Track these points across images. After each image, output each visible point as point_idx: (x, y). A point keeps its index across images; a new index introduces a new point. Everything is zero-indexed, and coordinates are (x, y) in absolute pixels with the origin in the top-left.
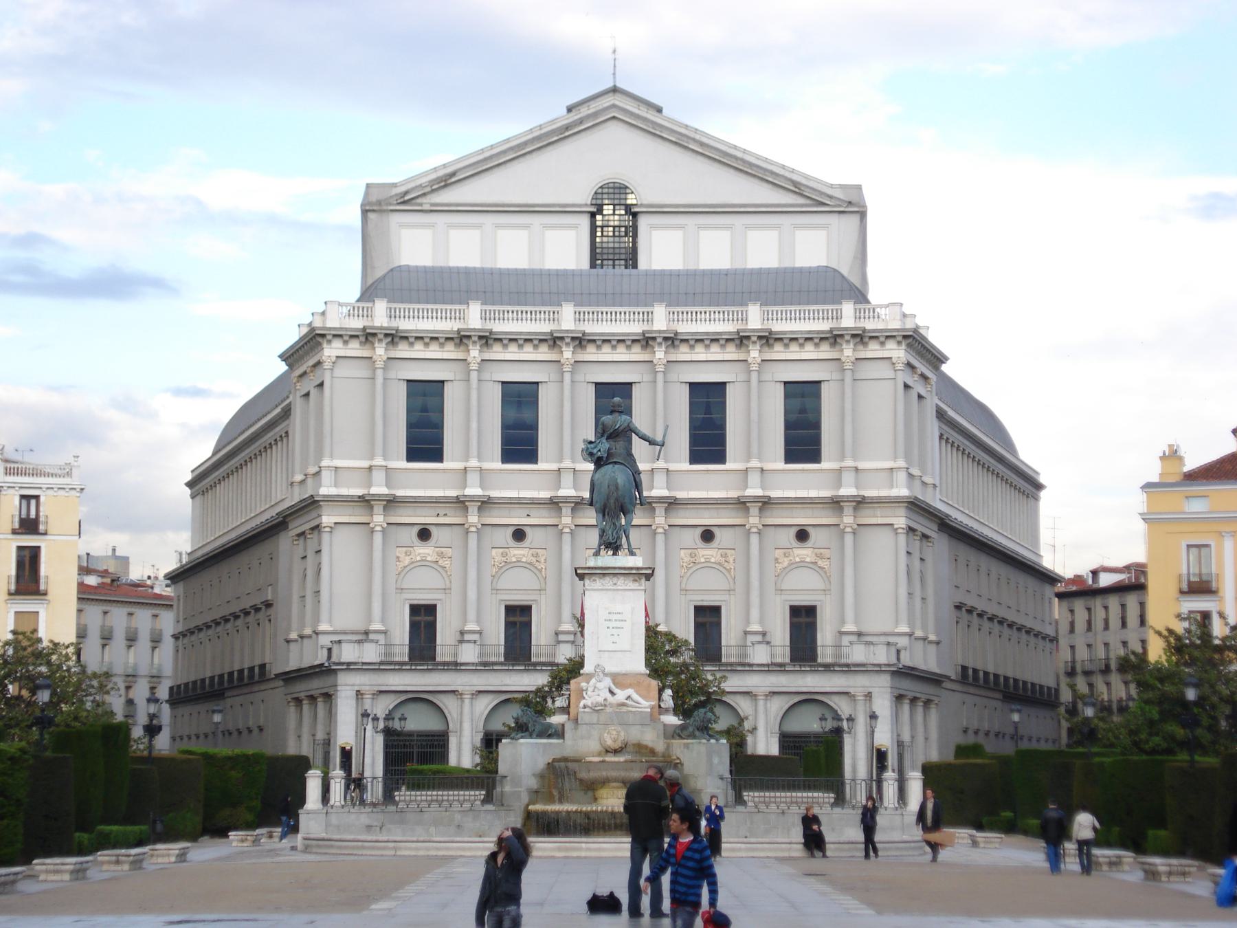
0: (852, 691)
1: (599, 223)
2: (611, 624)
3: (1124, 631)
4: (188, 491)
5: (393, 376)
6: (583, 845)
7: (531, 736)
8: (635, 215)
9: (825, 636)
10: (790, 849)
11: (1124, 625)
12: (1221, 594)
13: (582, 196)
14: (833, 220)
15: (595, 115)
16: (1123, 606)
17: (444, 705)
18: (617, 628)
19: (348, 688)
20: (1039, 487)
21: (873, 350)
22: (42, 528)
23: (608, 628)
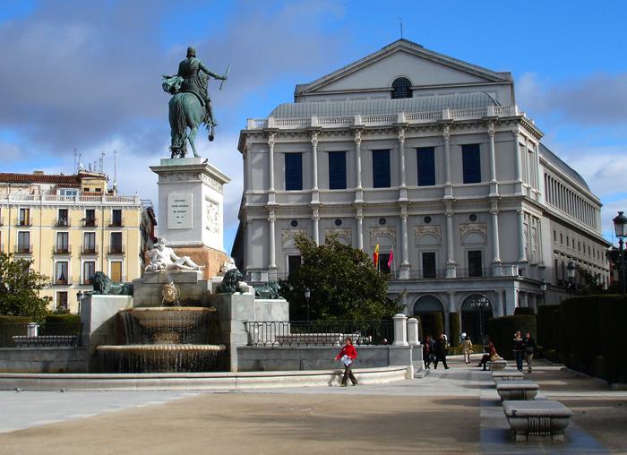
0: (496, 290)
6: (39, 381)
7: (101, 293)
9: (485, 264)
10: (236, 383)
13: (387, 82)
14: (499, 88)
15: (392, 50)
20: (600, 205)
21: (504, 128)
22: (122, 224)
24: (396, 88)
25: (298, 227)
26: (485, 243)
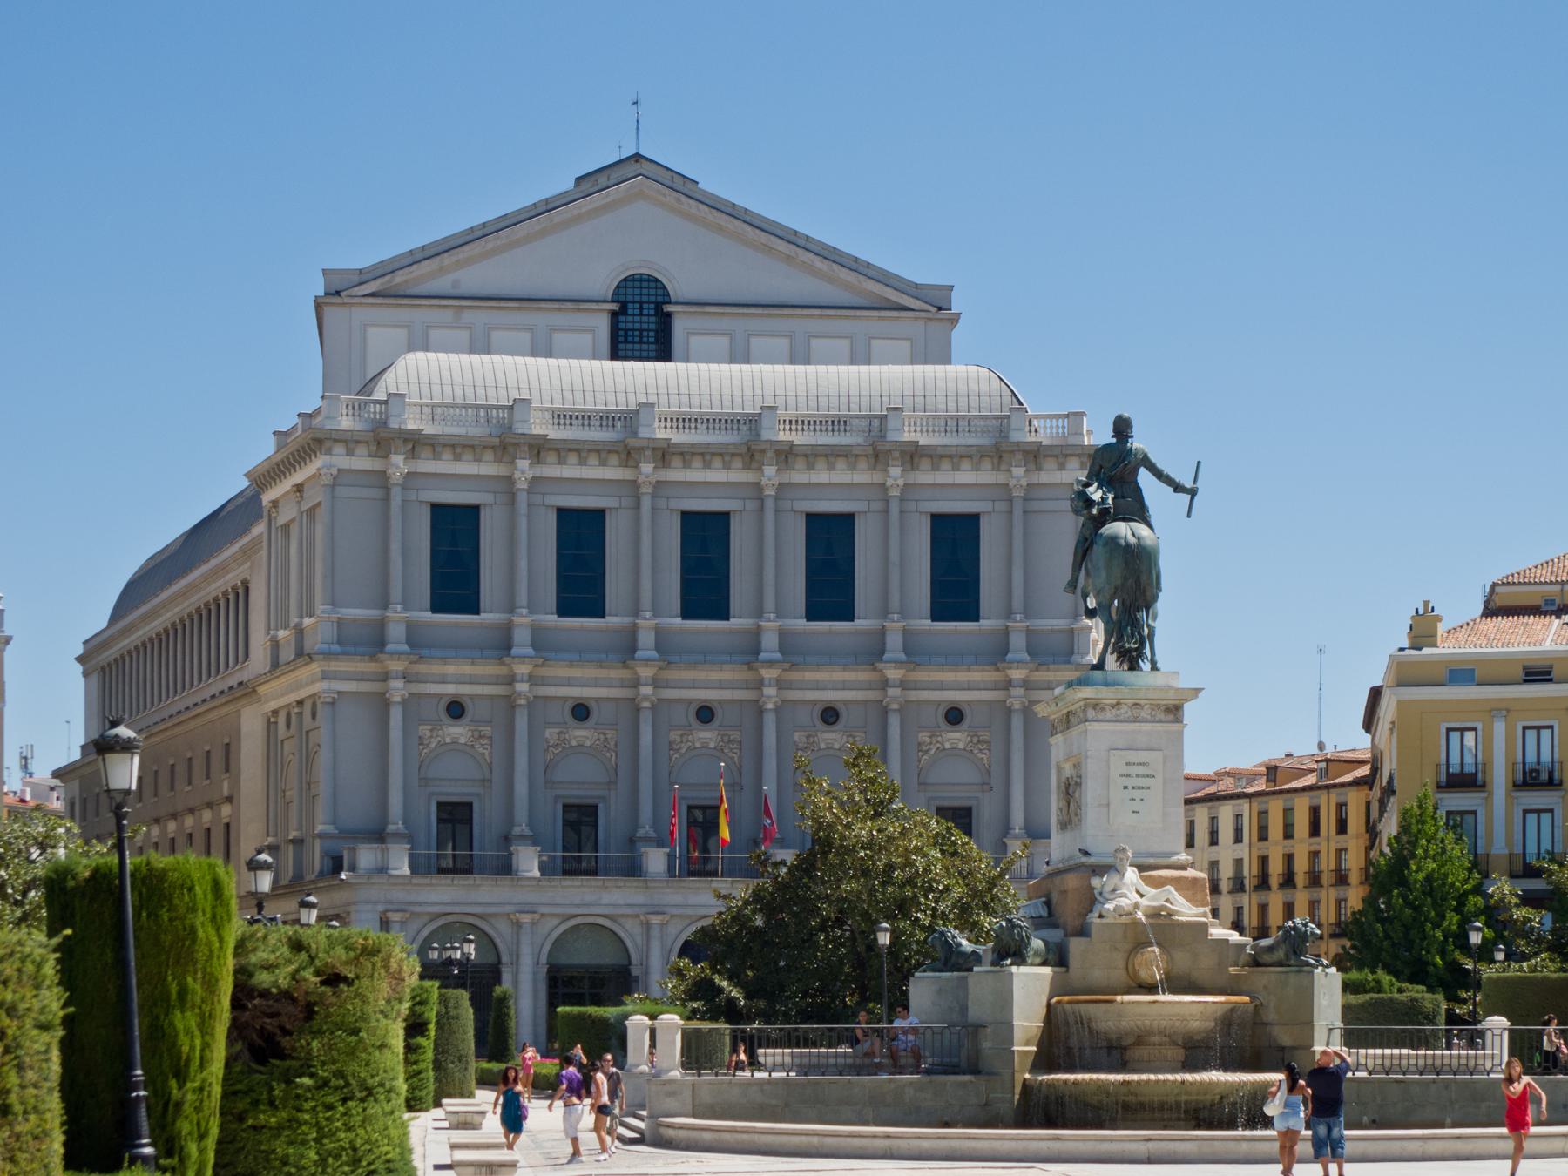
1: (622, 326)
2: (1130, 782)
3: (1214, 848)
4: (79, 668)
5: (414, 498)
8: (669, 315)
11: (1214, 841)
12: (1488, 788)
16: (1213, 820)
17: (496, 930)
18: (1139, 788)
19: (369, 907)
23: (1126, 788)
24: (623, 310)
25: (466, 719)
26: (985, 785)
